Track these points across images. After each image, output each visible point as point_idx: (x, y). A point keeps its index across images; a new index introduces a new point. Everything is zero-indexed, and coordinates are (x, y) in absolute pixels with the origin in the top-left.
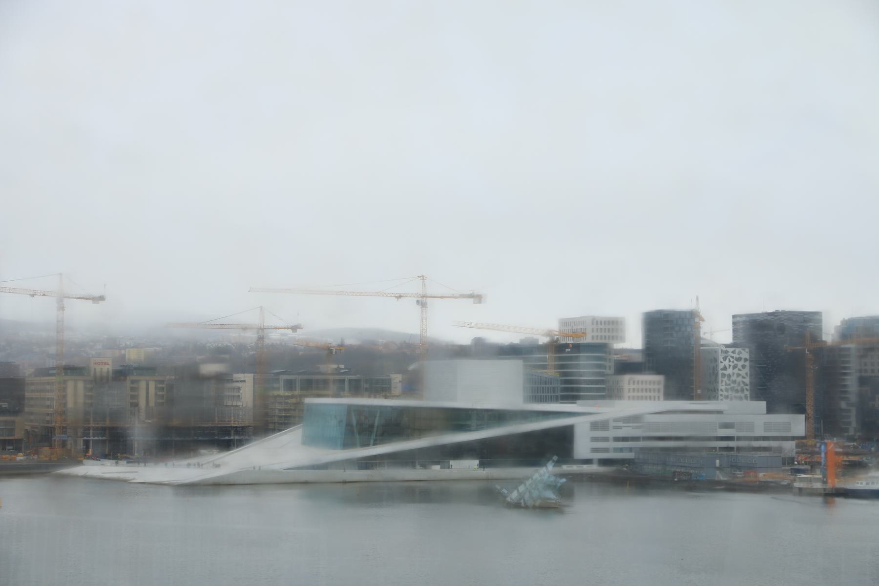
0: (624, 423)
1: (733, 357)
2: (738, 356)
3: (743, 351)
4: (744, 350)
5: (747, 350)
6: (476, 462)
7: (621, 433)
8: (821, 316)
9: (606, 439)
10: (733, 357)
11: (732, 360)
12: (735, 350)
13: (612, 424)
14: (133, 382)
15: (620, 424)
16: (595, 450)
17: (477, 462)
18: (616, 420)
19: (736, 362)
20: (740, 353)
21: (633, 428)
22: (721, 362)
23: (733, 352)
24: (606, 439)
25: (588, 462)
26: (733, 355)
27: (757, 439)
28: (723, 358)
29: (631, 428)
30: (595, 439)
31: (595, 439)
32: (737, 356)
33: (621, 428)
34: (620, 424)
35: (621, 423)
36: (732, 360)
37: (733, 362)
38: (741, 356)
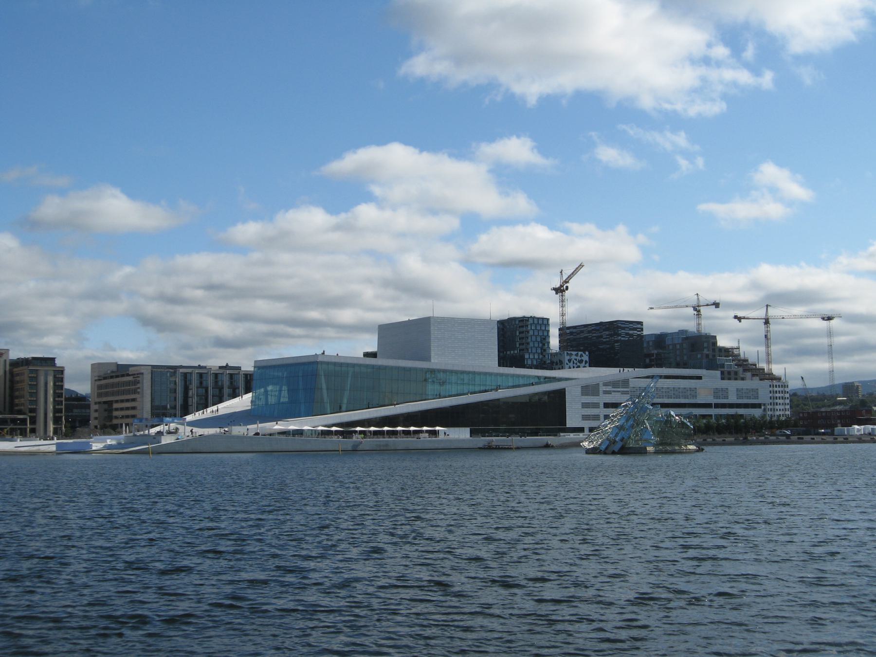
0: (613, 387)
1: (576, 360)
2: (580, 359)
3: (583, 354)
4: (585, 354)
5: (587, 353)
6: (468, 430)
7: (609, 399)
8: (642, 325)
9: (596, 405)
10: (576, 360)
11: (575, 362)
12: (578, 354)
13: (602, 388)
14: (32, 371)
15: (609, 388)
16: (585, 418)
17: (468, 430)
18: (605, 384)
19: (578, 364)
20: (581, 356)
21: (622, 394)
22: (567, 364)
23: (577, 355)
24: (596, 405)
25: (581, 430)
26: (576, 357)
27: (731, 406)
28: (568, 360)
29: (620, 393)
30: (585, 405)
31: (585, 405)
32: (579, 358)
33: (611, 393)
34: (609, 388)
35: (610, 387)
36: (575, 362)
37: (576, 364)
38: (582, 358)
